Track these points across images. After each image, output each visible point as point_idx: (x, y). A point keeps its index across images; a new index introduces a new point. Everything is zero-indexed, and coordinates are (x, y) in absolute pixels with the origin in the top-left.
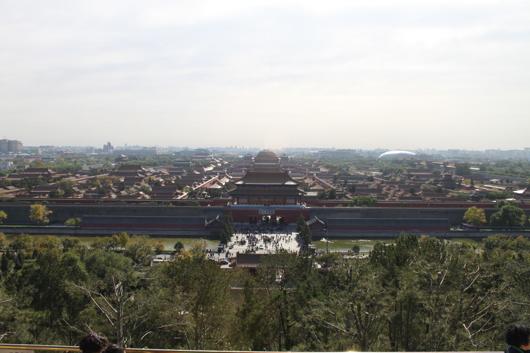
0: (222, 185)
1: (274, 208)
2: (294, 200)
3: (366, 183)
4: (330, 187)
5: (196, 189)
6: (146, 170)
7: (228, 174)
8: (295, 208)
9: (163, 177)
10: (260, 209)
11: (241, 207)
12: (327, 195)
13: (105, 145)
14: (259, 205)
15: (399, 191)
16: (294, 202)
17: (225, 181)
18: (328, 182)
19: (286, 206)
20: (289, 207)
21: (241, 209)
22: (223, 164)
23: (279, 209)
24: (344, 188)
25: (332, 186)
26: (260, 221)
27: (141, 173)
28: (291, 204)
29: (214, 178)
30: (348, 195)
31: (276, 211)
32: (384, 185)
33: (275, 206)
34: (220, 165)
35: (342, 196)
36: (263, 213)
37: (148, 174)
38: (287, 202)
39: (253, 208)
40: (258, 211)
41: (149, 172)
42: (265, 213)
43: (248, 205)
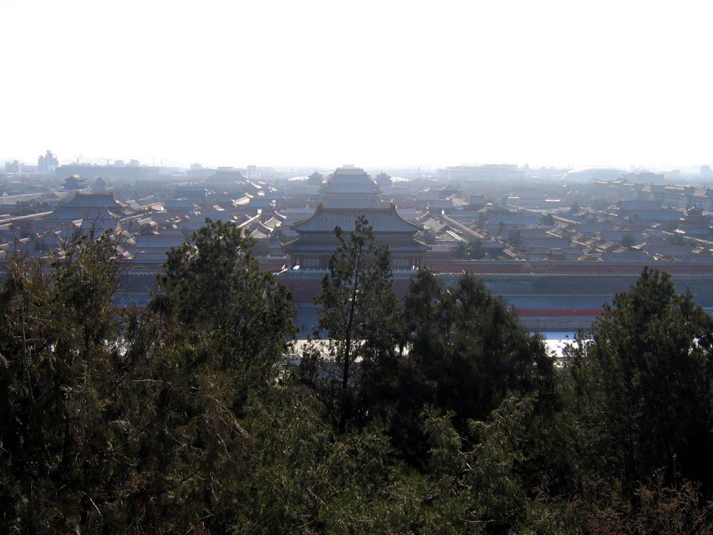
0: (267, 232)
3: (539, 227)
4: (471, 235)
6: (124, 205)
9: (155, 215)
11: (309, 274)
12: (469, 251)
13: (42, 157)
15: (602, 242)
18: (468, 226)
22: (267, 192)
24: (499, 238)
27: (112, 209)
29: (252, 219)
30: (507, 251)
32: (574, 231)
34: (261, 194)
35: (498, 252)
37: (127, 212)
41: (129, 208)
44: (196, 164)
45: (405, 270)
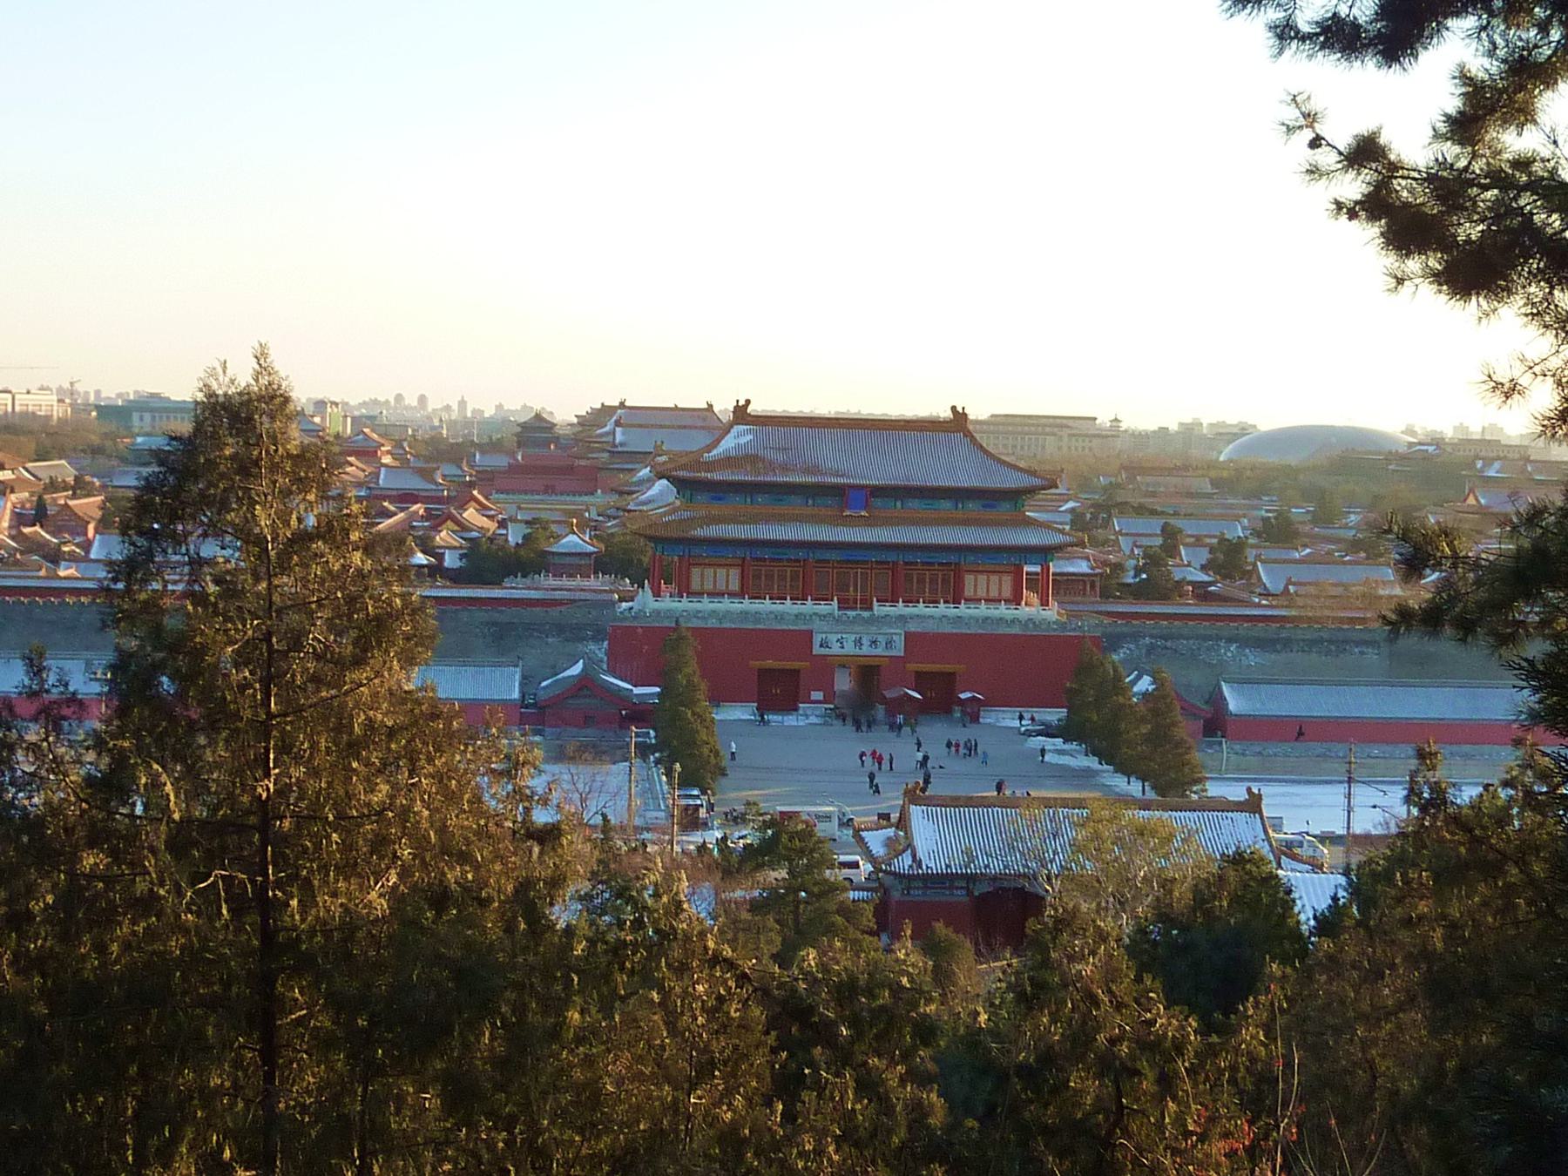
1: (902, 619)
19: (964, 610)
23: (931, 627)
26: (817, 695)
31: (909, 636)
33: (901, 608)
36: (835, 649)
39: (780, 617)
43: (747, 605)
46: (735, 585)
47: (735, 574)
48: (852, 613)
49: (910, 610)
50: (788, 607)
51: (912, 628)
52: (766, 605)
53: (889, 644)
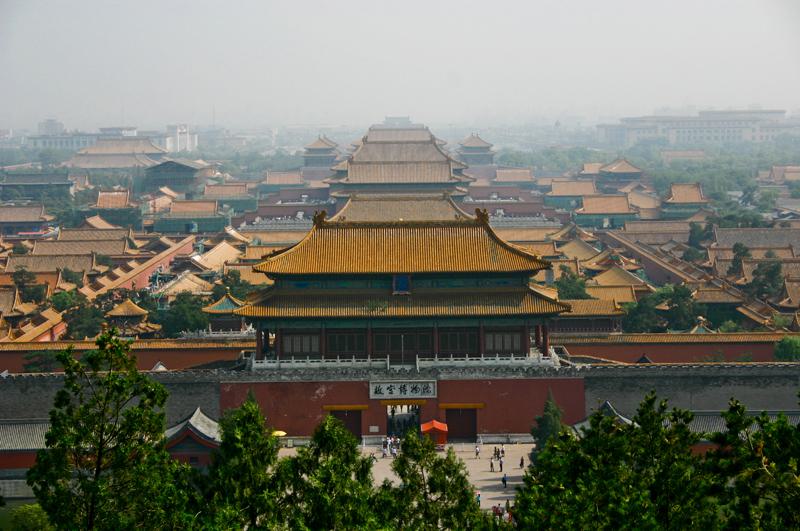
1: (434, 371)
2: (517, 337)
4: (670, 277)
5: (102, 297)
7: (236, 227)
8: (520, 368)
10: (374, 377)
11: (296, 371)
14: (368, 362)
16: (517, 346)
17: (219, 257)
19: (484, 361)
20: (498, 368)
21: (296, 378)
23: (455, 375)
25: (678, 271)
26: (374, 429)
28: (505, 354)
31: (441, 384)
33: (437, 362)
36: (386, 395)
38: (490, 346)
39: (345, 372)
40: (364, 388)
42: (397, 394)
43: (324, 363)
44: (51, 123)
45: (513, 358)
46: (315, 349)
47: (315, 341)
48: (397, 367)
49: (444, 363)
50: (354, 363)
51: (443, 376)
52: (339, 363)
53: (426, 390)
